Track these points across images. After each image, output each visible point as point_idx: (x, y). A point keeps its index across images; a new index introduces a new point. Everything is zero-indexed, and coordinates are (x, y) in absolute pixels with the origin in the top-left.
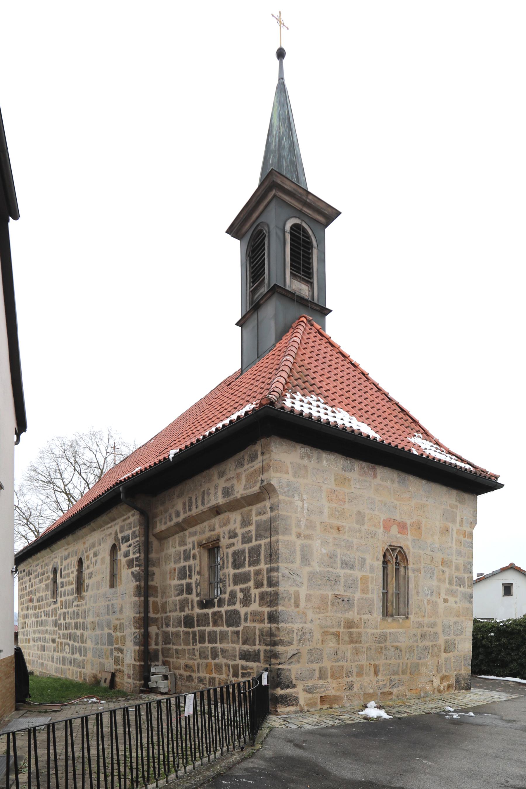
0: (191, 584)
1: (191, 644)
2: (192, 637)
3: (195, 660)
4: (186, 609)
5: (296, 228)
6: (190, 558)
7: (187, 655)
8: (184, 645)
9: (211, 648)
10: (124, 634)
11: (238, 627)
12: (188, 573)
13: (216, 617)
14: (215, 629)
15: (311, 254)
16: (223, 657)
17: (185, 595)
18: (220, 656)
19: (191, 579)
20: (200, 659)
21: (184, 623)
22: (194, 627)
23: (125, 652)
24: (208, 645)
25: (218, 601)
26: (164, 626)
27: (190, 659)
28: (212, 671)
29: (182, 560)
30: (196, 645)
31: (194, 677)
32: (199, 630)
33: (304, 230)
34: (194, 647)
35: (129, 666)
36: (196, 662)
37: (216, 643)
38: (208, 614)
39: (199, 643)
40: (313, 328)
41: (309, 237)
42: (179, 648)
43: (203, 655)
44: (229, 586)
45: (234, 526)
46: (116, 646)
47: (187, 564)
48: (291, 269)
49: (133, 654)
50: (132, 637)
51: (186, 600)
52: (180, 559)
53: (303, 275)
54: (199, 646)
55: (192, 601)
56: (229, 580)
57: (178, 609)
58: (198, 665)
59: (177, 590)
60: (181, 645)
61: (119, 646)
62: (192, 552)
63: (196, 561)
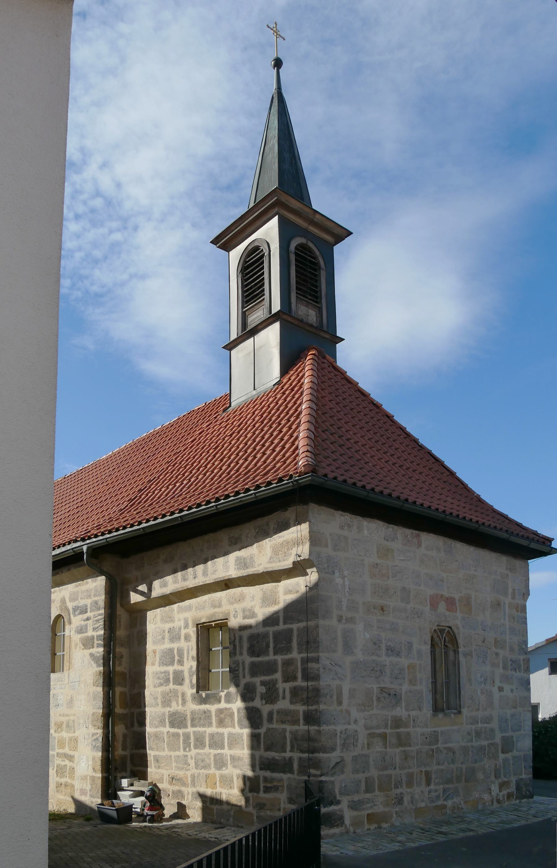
0: (182, 672)
1: (182, 750)
2: (184, 740)
3: (188, 770)
4: (174, 704)
5: (301, 248)
6: (180, 638)
7: (174, 764)
8: (170, 750)
9: (215, 755)
10: (76, 735)
11: (259, 728)
12: (177, 658)
13: (222, 716)
14: (221, 730)
15: (319, 275)
16: (234, 767)
17: (171, 686)
18: (229, 766)
19: (182, 665)
20: (196, 768)
21: (170, 722)
22: (186, 727)
23: (76, 759)
24: (209, 752)
25: (225, 696)
26: (136, 724)
27: (179, 769)
28: (215, 784)
29: (166, 640)
30: (190, 750)
31: (186, 793)
32: (194, 732)
33: (310, 250)
34: (186, 753)
35: (84, 778)
36: (189, 773)
37: (222, 748)
38: (210, 711)
39: (195, 748)
40: (325, 361)
41: (315, 258)
42: (162, 754)
43: (201, 764)
44: (244, 677)
45: (252, 604)
46: (61, 751)
47: (175, 646)
48: (297, 293)
49: (91, 763)
50: (90, 741)
51: (175, 693)
52: (163, 638)
53: (310, 299)
54: (194, 752)
55: (183, 695)
56: (244, 669)
57: (160, 703)
58: (193, 776)
59: (158, 678)
60: (164, 750)
61: (67, 750)
62: (183, 632)
63: (190, 644)
